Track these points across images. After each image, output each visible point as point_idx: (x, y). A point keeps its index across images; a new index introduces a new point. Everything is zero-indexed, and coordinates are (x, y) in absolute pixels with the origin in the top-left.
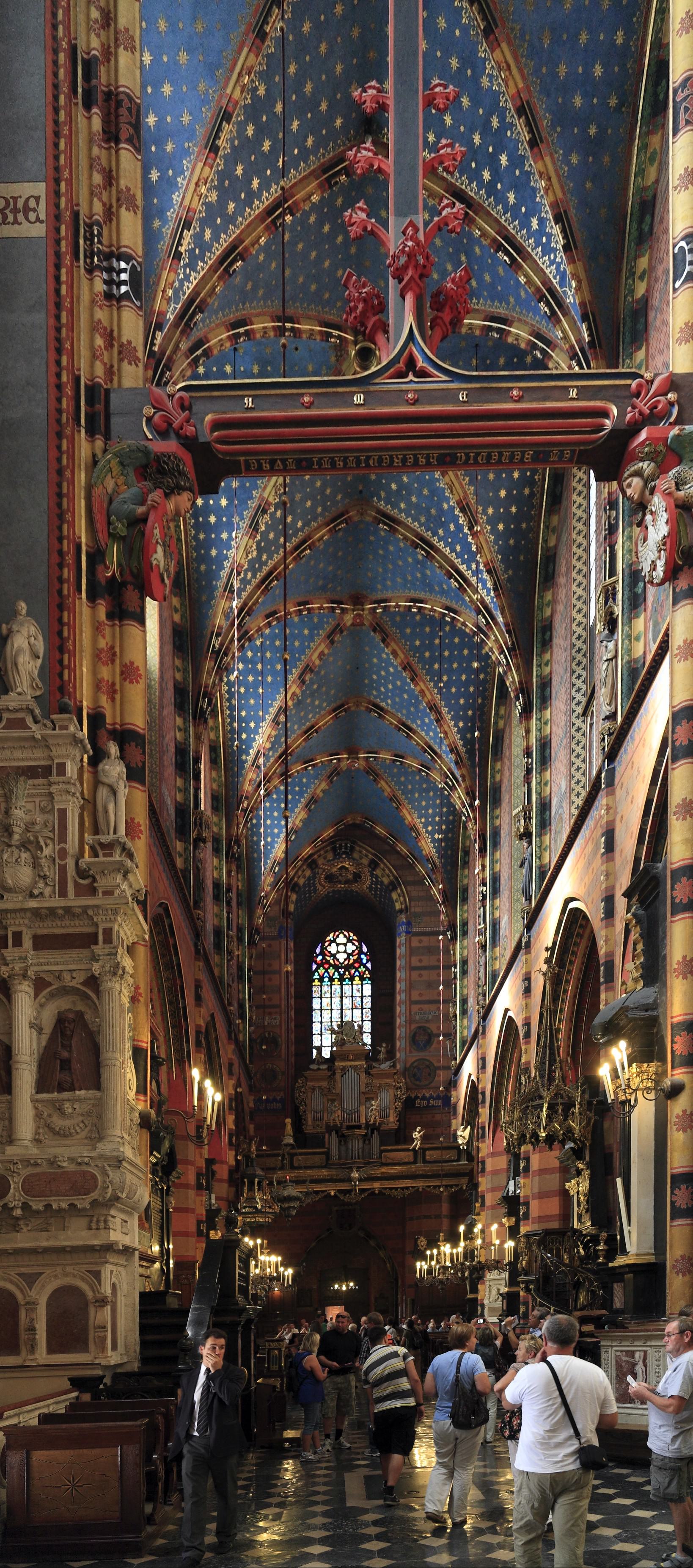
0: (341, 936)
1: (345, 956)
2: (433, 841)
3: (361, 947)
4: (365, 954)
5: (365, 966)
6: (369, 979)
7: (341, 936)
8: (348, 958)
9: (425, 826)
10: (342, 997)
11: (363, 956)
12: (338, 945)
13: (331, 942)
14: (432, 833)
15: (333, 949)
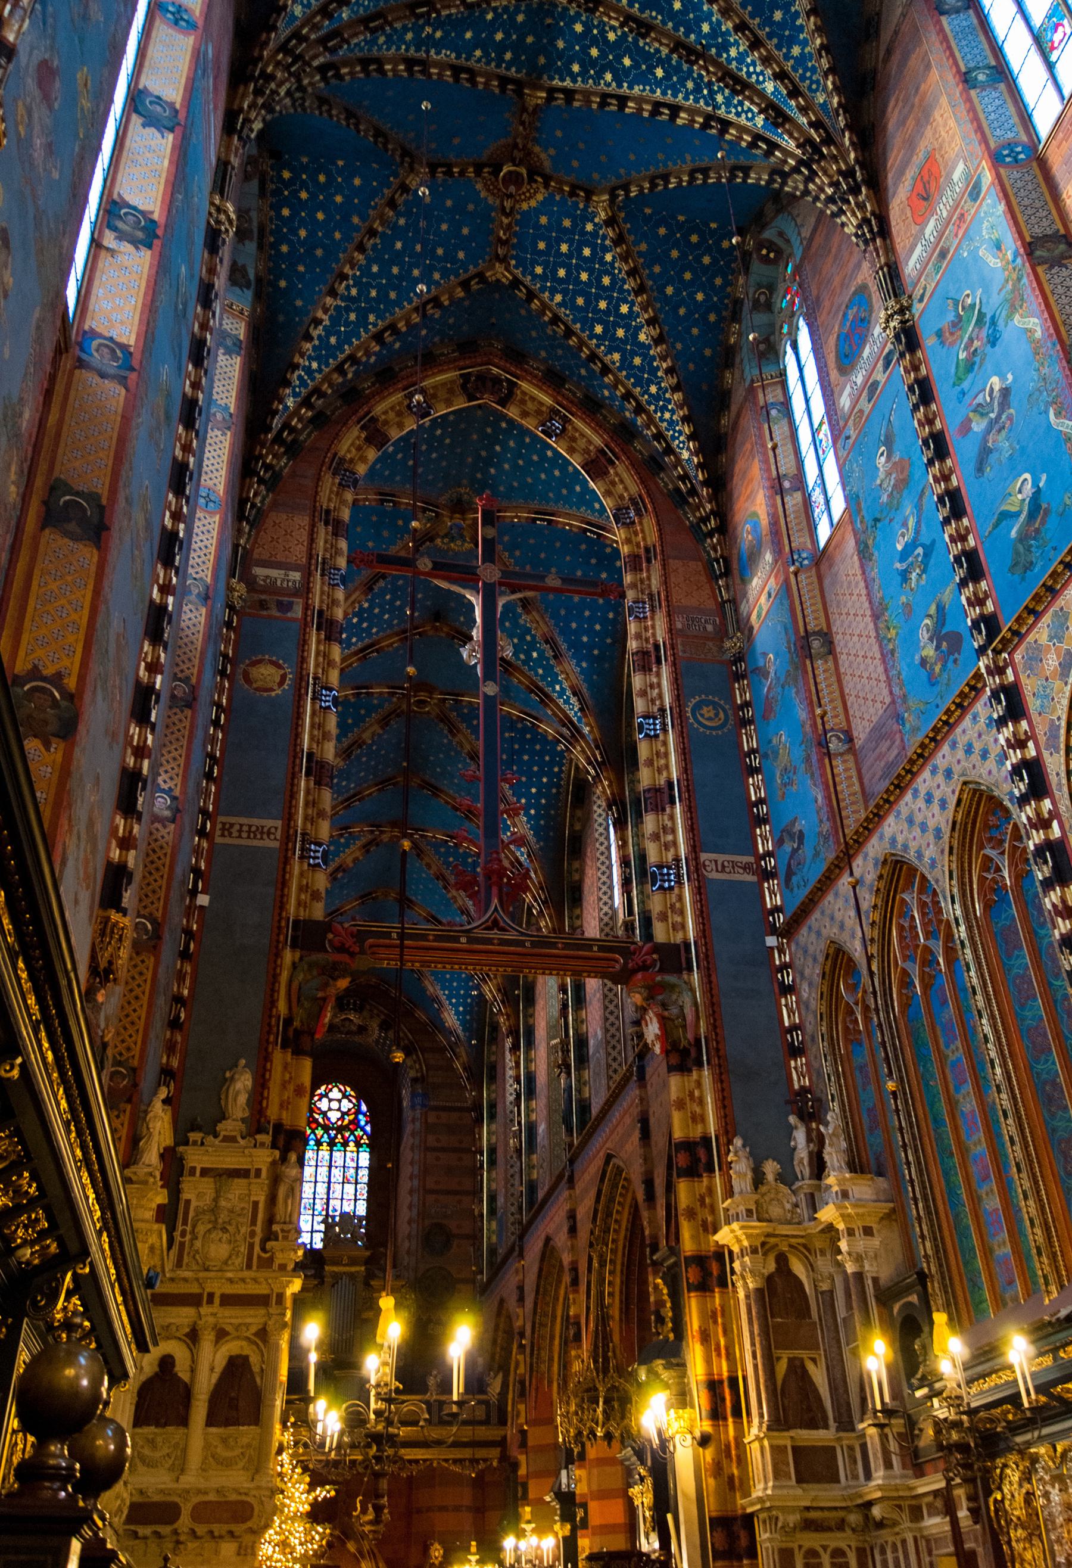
0: (335, 1090)
1: (339, 1115)
2: (457, 1013)
3: (359, 1106)
4: (365, 1115)
5: (363, 1129)
6: (368, 1145)
7: (335, 1090)
8: (342, 1118)
9: (449, 998)
10: (330, 1167)
11: (361, 1117)
12: (330, 1100)
13: (321, 1096)
14: (456, 1006)
15: (324, 1105)
